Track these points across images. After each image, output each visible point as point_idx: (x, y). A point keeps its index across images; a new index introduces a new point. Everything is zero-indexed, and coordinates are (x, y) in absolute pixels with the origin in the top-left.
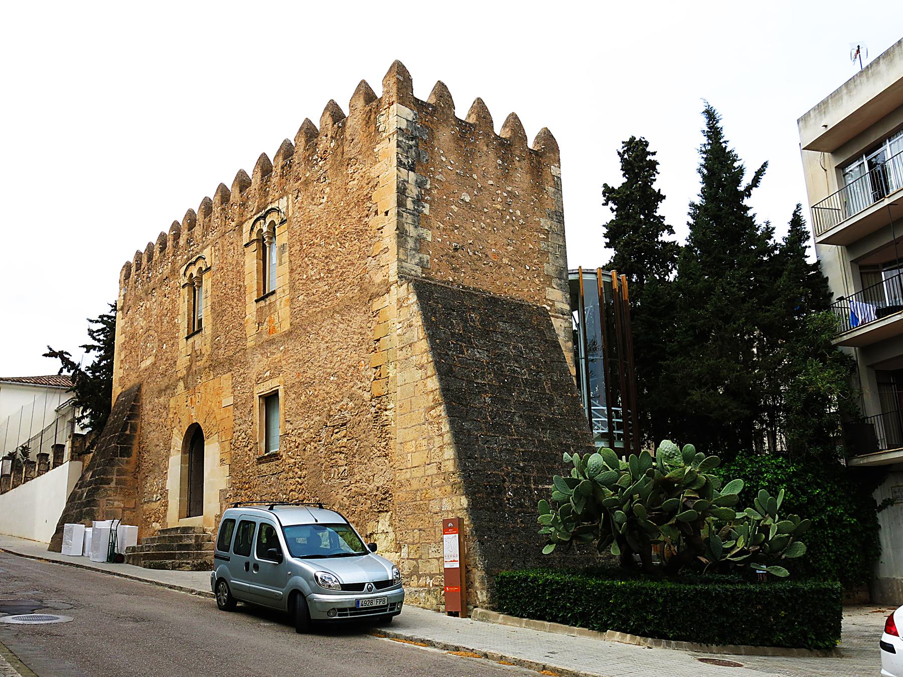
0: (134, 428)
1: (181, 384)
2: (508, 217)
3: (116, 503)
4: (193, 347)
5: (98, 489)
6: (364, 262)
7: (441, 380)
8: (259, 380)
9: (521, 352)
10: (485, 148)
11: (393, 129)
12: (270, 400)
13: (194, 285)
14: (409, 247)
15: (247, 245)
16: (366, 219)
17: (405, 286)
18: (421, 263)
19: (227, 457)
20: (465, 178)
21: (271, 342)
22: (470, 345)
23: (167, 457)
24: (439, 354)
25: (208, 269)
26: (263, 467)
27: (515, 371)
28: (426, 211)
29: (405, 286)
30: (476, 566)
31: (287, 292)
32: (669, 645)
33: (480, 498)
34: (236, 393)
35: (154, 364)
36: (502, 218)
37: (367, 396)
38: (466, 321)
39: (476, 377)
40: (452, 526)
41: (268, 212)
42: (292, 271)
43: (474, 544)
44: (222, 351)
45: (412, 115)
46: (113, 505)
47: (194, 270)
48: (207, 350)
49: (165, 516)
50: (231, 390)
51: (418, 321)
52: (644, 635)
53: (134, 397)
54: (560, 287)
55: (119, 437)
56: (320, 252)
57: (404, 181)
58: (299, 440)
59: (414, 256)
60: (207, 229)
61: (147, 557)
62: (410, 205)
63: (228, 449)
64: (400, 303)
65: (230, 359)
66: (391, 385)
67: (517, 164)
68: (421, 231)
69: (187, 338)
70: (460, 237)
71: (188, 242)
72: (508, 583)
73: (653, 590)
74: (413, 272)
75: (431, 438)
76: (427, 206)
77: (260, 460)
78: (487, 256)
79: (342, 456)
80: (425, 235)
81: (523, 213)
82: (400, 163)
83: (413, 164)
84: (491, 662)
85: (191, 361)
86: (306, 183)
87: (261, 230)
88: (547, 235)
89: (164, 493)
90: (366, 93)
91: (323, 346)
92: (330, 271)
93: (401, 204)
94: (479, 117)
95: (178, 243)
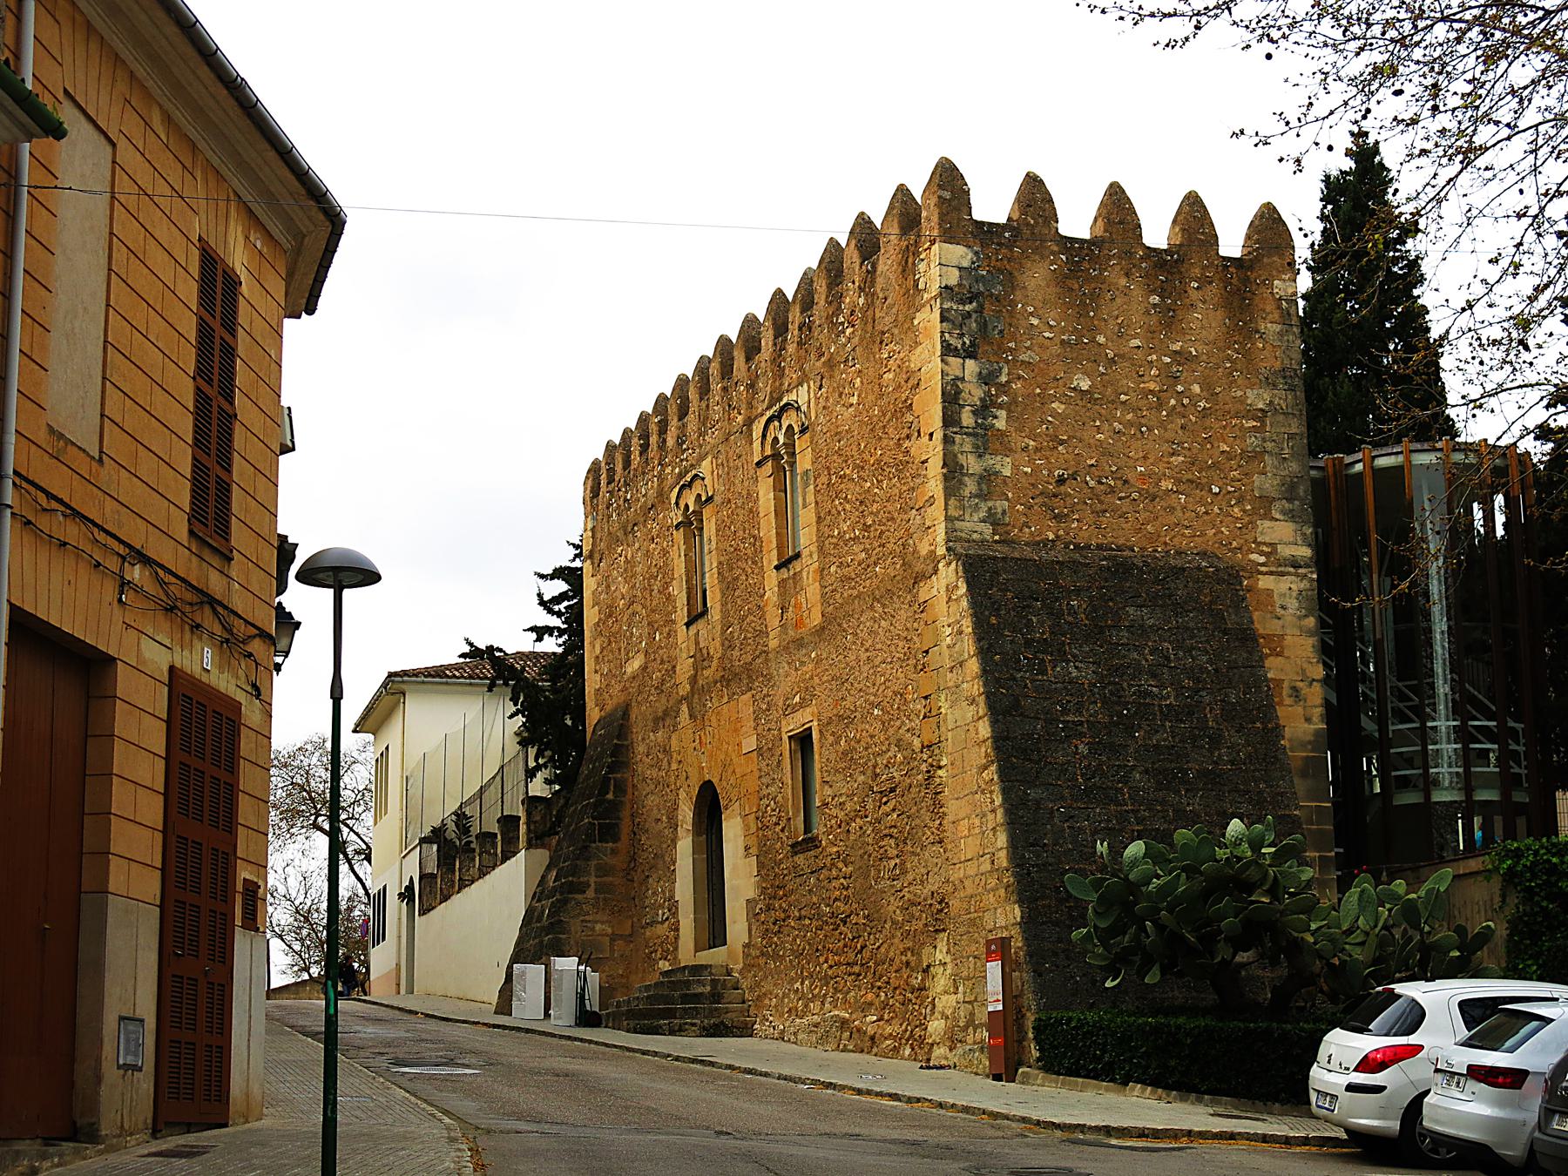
0: (620, 789)
1: (684, 708)
2: (1173, 402)
3: (598, 927)
4: (697, 643)
5: (565, 902)
6: (906, 517)
7: (994, 723)
8: (789, 710)
9: (1167, 658)
10: (1123, 281)
11: (934, 289)
12: (803, 741)
13: (691, 524)
14: (967, 493)
15: (759, 464)
16: (907, 444)
17: (953, 565)
18: (992, 519)
19: (753, 841)
20: (1078, 351)
21: (799, 643)
22: (1062, 656)
23: (674, 841)
24: (997, 680)
25: (710, 499)
26: (800, 859)
27: (1148, 694)
28: (1000, 424)
29: (953, 565)
30: (1029, 1009)
31: (815, 557)
32: (1199, 1101)
33: (1044, 906)
34: (760, 728)
35: (644, 668)
36: (1160, 404)
37: (917, 743)
38: (1060, 615)
39: (1065, 711)
40: (999, 949)
41: (783, 409)
42: (819, 520)
43: (1023, 977)
44: (736, 653)
45: (970, 255)
46: (593, 929)
47: (690, 499)
48: (716, 649)
49: (676, 949)
50: (752, 724)
51: (967, 626)
52: (1168, 1087)
53: (619, 724)
54: (1291, 516)
55: (595, 805)
56: (853, 491)
57: (957, 378)
58: (841, 815)
59: (977, 508)
60: (704, 420)
61: (632, 1014)
62: (967, 419)
63: (754, 829)
64: (950, 589)
65: (747, 667)
66: (943, 729)
67: (1194, 295)
68: (990, 461)
69: (688, 625)
70: (1070, 457)
71: (680, 441)
72: (1046, 1027)
73: (1179, 1027)
74: (975, 536)
75: (985, 815)
76: (1002, 414)
77: (798, 848)
78: (1126, 482)
79: (892, 842)
80: (998, 467)
81: (1207, 386)
82: (947, 350)
83: (973, 344)
84: (942, 1112)
85: (695, 667)
86: (831, 365)
87: (776, 439)
88: (1262, 420)
89: (674, 908)
90: (901, 214)
91: (864, 656)
92: (866, 528)
93: (950, 420)
94: (1109, 223)
95: (665, 441)
